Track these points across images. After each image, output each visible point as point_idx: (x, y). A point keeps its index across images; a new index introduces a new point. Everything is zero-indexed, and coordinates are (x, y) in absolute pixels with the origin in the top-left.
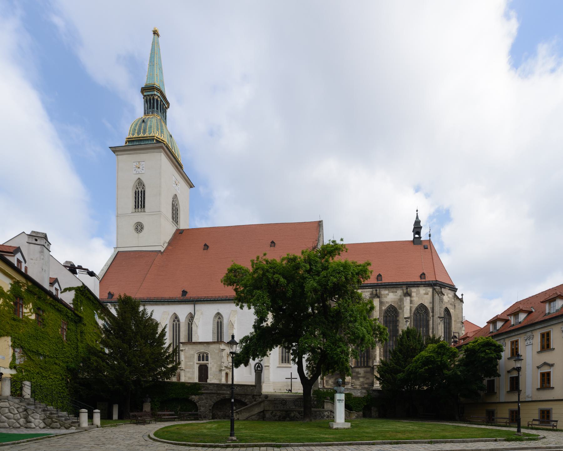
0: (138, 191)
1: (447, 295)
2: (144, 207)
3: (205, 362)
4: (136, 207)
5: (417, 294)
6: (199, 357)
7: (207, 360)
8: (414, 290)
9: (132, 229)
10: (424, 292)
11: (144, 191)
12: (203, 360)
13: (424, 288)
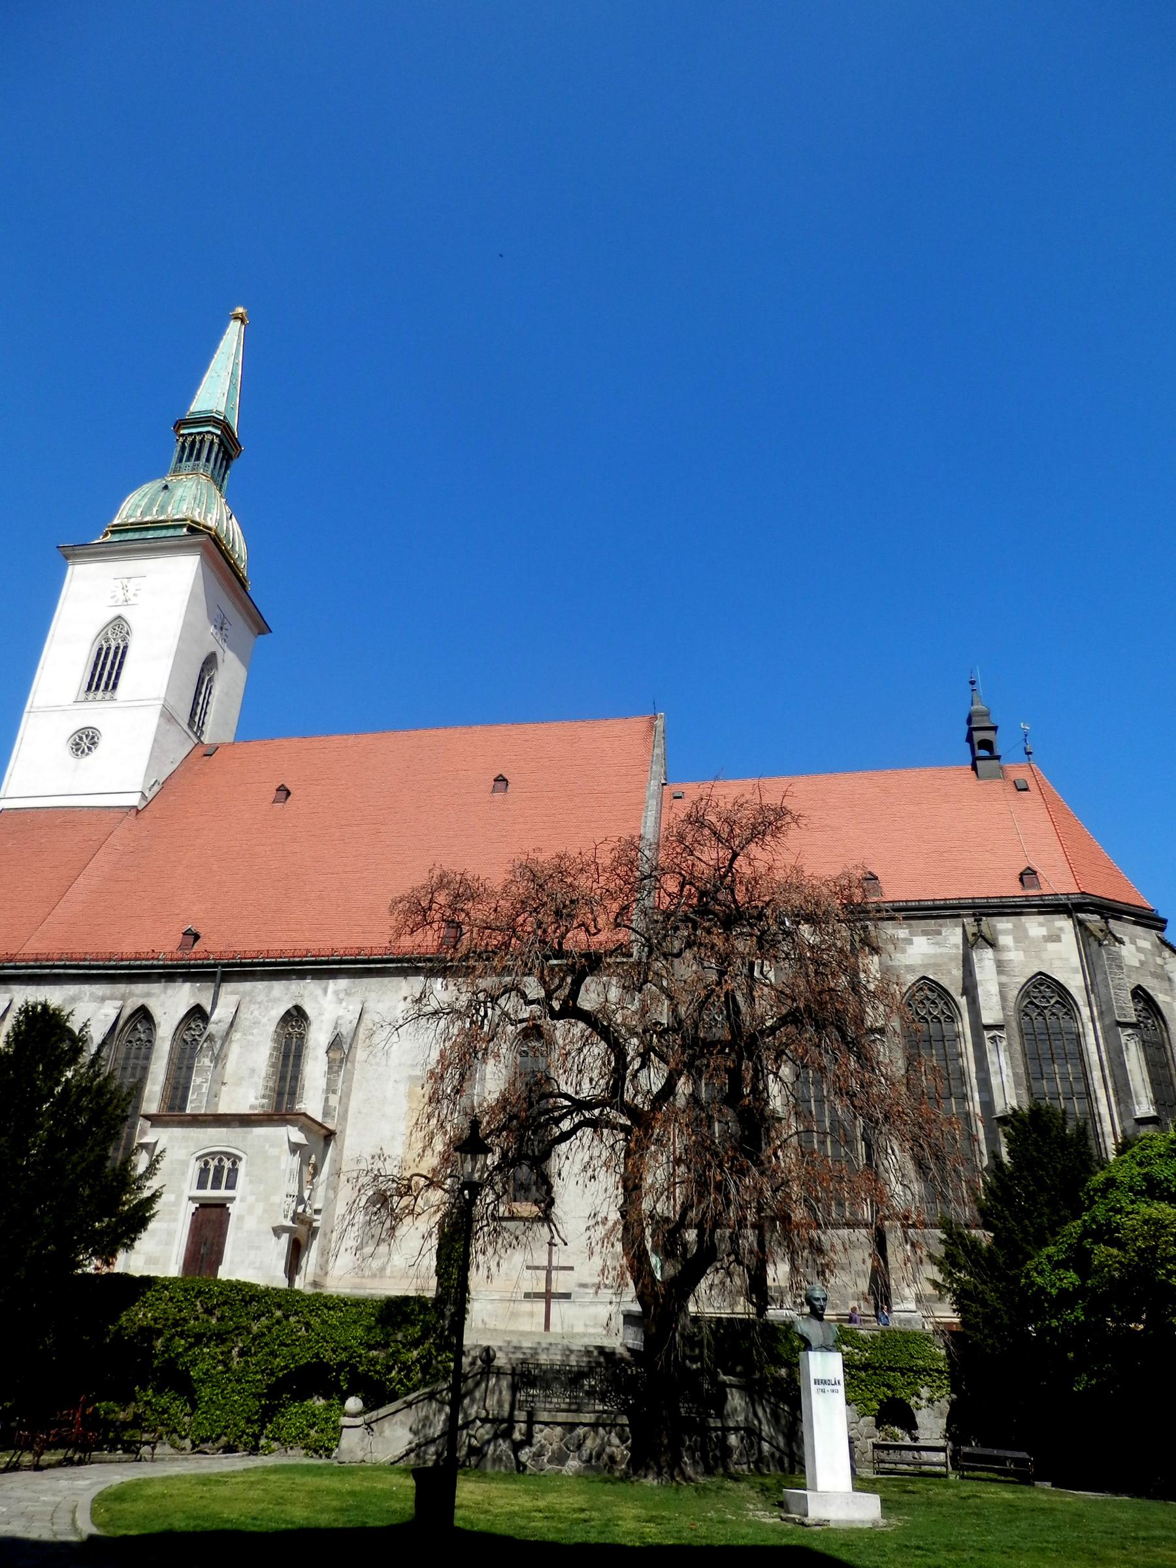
0: (109, 649)
1: (1133, 942)
2: (115, 686)
3: (222, 1193)
4: (93, 685)
5: (1017, 940)
6: (204, 1171)
7: (231, 1186)
8: (1003, 925)
9: (63, 749)
10: (1043, 931)
11: (126, 647)
12: (216, 1185)
13: (1041, 918)
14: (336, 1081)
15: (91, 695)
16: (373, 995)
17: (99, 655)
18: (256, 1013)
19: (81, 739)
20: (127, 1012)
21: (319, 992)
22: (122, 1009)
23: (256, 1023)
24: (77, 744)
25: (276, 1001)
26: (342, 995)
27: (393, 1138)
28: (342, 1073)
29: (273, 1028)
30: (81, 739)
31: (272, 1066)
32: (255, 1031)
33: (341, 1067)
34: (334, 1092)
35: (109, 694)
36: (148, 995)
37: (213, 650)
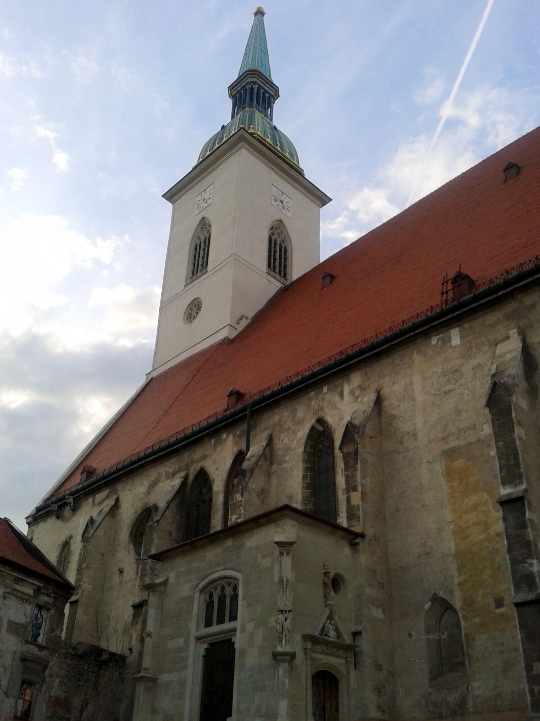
0: (201, 243)
11: (210, 236)
14: (354, 476)
15: (194, 278)
16: (387, 380)
17: (196, 249)
18: (286, 440)
19: (192, 309)
20: (191, 478)
21: (337, 398)
22: (186, 477)
23: (288, 449)
24: (190, 314)
25: (301, 422)
26: (357, 393)
27: (440, 530)
28: (359, 466)
29: (301, 450)
30: (192, 309)
31: (307, 488)
32: (287, 458)
33: (356, 460)
34: (355, 489)
35: (204, 271)
36: (204, 457)
37: (278, 217)
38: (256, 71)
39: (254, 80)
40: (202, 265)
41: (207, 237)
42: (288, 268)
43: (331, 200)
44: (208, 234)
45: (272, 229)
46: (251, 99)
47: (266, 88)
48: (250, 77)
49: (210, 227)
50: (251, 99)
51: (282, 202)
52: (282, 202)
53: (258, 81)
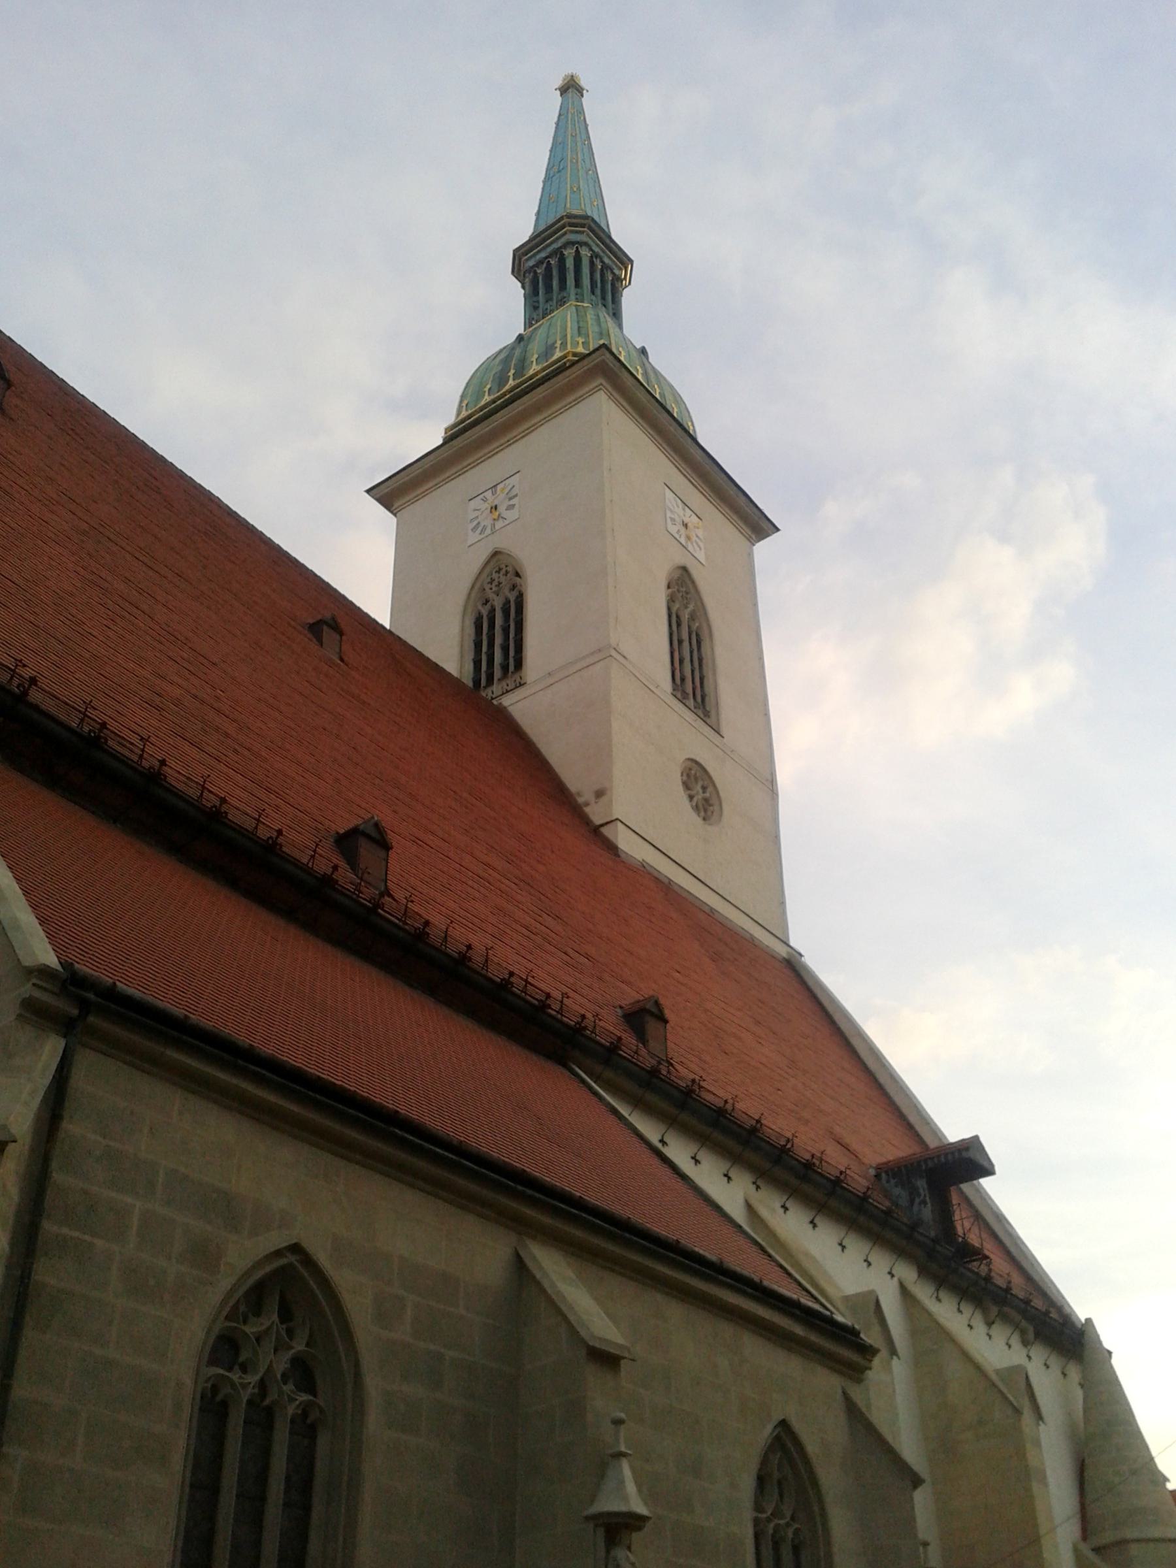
0: (493, 610)
38: (587, 217)
39: (583, 238)
40: (505, 668)
41: (512, 600)
42: (708, 683)
43: (778, 530)
44: (515, 593)
45: (669, 587)
46: (578, 283)
47: (606, 260)
48: (572, 232)
49: (518, 575)
50: (578, 283)
51: (686, 526)
52: (686, 526)
53: (590, 242)
